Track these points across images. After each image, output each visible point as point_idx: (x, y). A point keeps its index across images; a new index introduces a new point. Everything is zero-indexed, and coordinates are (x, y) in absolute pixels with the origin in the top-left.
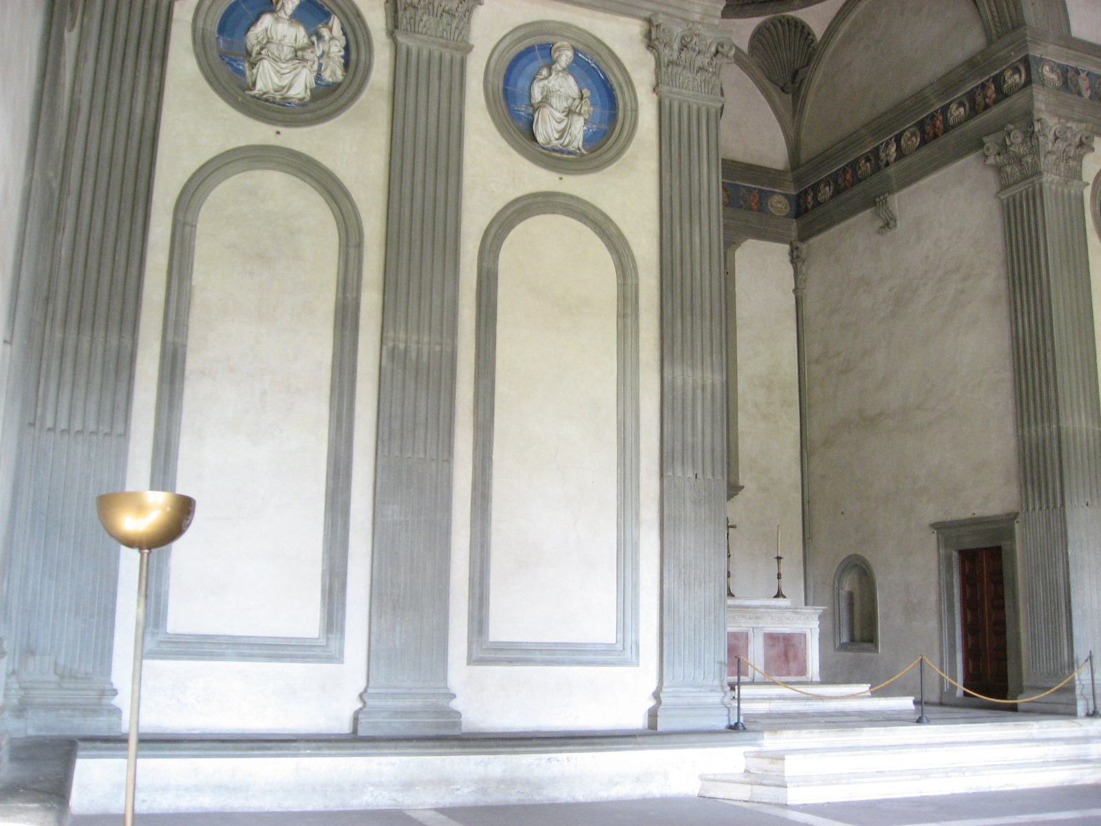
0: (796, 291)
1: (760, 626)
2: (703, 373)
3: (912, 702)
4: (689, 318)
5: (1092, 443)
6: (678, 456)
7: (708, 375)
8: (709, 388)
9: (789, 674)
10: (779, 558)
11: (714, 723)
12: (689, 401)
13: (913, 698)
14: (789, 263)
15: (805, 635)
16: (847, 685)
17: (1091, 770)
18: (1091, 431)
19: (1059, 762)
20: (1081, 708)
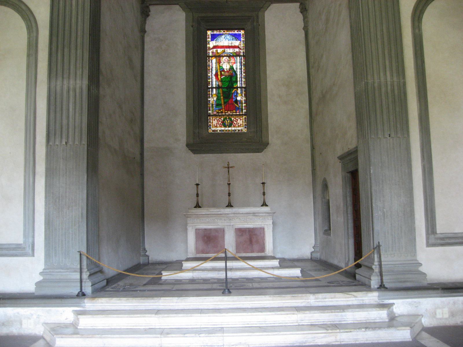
0: (304, 29)
1: (231, 224)
2: (56, 82)
3: (300, 271)
4: (66, 50)
5: (396, 92)
6: (58, 133)
7: (78, 82)
8: (78, 91)
9: (252, 252)
10: (263, 183)
11: (72, 291)
12: (65, 99)
13: (300, 269)
14: (300, 13)
15: (264, 229)
16: (261, 261)
17: (323, 335)
18: (395, 84)
19: (299, 327)
20: (375, 282)
